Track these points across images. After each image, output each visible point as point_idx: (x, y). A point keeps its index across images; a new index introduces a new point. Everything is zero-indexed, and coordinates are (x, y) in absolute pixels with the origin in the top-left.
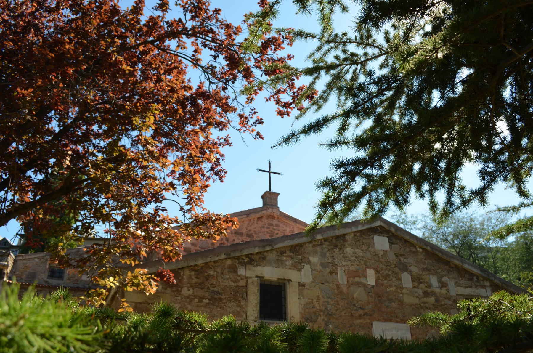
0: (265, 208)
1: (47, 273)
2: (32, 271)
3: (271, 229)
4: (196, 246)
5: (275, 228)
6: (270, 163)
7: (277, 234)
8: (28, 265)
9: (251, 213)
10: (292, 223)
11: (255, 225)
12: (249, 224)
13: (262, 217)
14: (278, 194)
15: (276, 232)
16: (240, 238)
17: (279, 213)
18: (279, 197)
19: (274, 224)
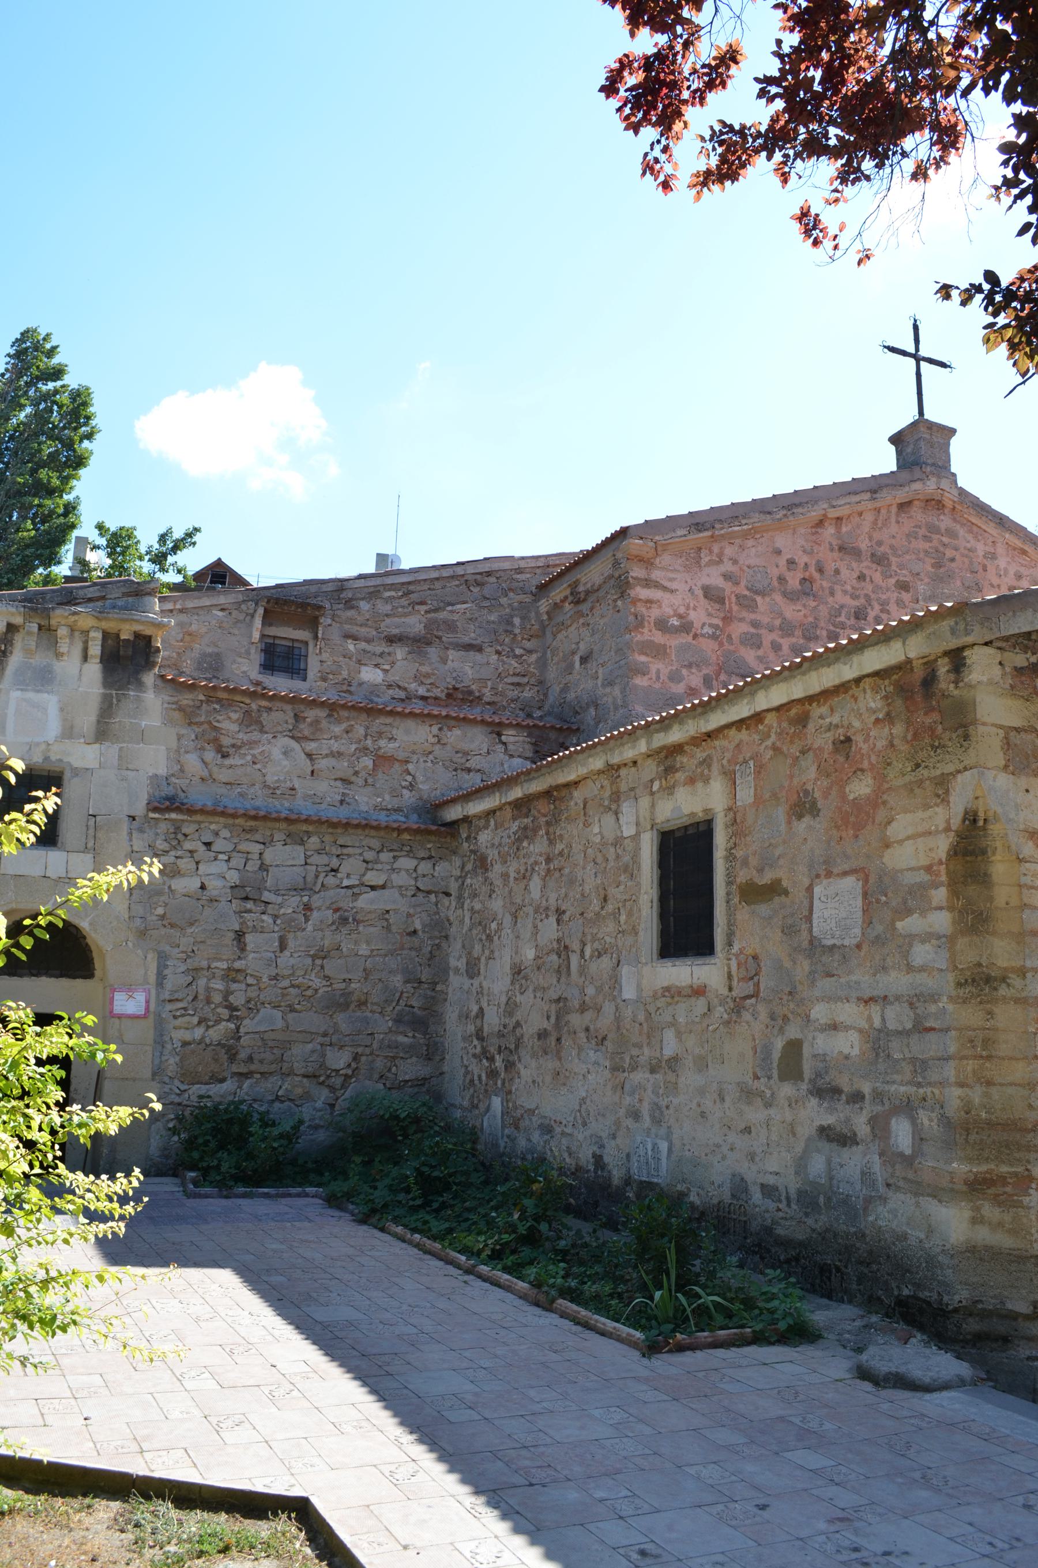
0: (905, 475)
1: (257, 657)
2: (210, 650)
3: (935, 543)
4: (737, 584)
5: (945, 540)
6: (916, 328)
7: (953, 560)
8: (194, 627)
9: (881, 488)
10: (991, 529)
11: (894, 529)
12: (875, 522)
13: (910, 502)
14: (953, 431)
15: (949, 553)
16: (854, 565)
17: (955, 493)
18: (954, 442)
19: (943, 526)
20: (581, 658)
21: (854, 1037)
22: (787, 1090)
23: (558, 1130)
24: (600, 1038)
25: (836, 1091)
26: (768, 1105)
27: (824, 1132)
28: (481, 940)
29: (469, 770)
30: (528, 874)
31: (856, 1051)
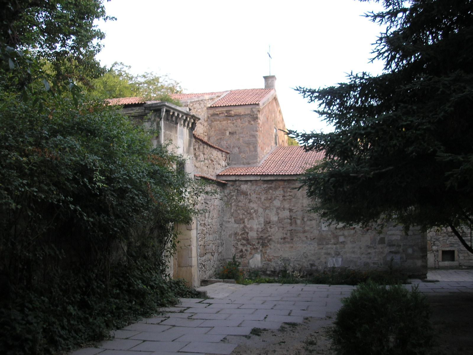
20: (230, 133)
21: (399, 237)
22: (380, 246)
23: (292, 260)
24: (312, 238)
25: (394, 245)
26: (375, 249)
27: (391, 252)
28: (244, 214)
29: (219, 164)
30: (273, 199)
31: (399, 238)
